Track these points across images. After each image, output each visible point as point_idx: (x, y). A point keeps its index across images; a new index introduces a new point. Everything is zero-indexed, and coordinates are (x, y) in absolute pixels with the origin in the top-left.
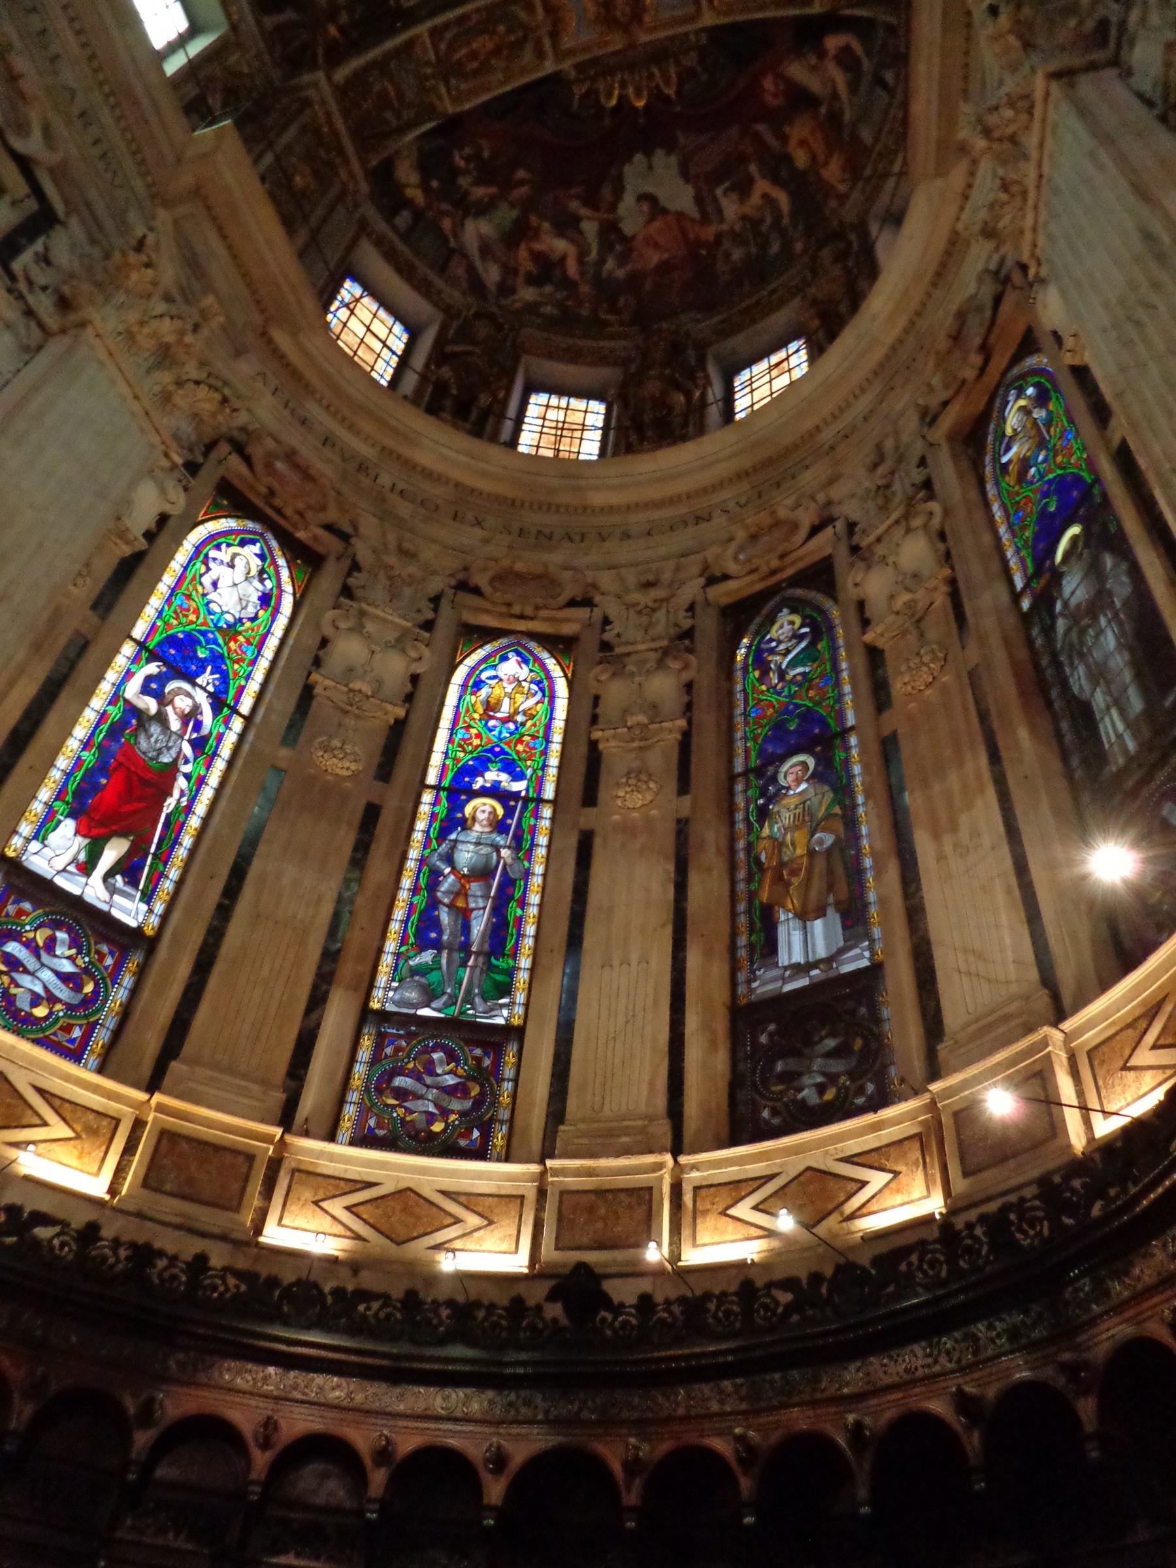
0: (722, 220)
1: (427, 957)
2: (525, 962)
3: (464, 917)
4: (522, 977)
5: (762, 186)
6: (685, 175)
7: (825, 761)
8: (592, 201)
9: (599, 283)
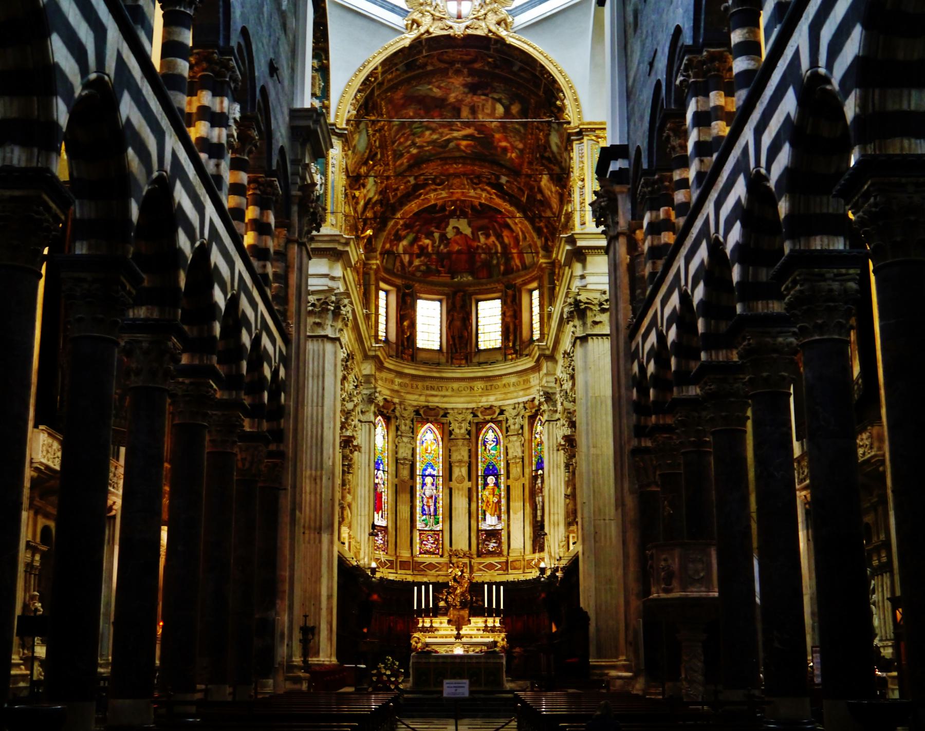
0: (479, 241)
1: (424, 517)
2: (441, 517)
3: (429, 507)
4: (441, 520)
5: (493, 239)
6: (469, 224)
7: (497, 479)
8: (438, 227)
9: (438, 253)
